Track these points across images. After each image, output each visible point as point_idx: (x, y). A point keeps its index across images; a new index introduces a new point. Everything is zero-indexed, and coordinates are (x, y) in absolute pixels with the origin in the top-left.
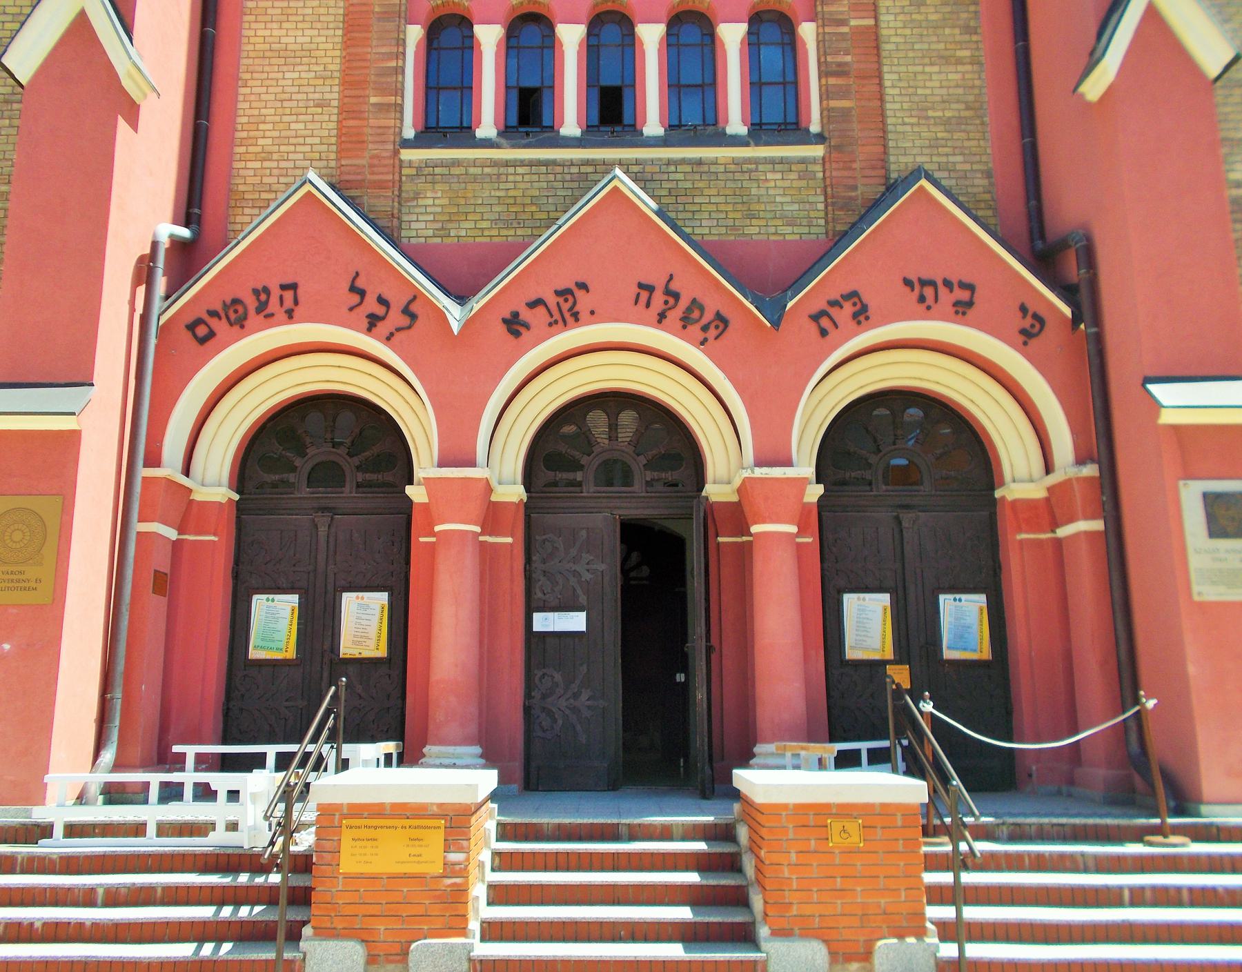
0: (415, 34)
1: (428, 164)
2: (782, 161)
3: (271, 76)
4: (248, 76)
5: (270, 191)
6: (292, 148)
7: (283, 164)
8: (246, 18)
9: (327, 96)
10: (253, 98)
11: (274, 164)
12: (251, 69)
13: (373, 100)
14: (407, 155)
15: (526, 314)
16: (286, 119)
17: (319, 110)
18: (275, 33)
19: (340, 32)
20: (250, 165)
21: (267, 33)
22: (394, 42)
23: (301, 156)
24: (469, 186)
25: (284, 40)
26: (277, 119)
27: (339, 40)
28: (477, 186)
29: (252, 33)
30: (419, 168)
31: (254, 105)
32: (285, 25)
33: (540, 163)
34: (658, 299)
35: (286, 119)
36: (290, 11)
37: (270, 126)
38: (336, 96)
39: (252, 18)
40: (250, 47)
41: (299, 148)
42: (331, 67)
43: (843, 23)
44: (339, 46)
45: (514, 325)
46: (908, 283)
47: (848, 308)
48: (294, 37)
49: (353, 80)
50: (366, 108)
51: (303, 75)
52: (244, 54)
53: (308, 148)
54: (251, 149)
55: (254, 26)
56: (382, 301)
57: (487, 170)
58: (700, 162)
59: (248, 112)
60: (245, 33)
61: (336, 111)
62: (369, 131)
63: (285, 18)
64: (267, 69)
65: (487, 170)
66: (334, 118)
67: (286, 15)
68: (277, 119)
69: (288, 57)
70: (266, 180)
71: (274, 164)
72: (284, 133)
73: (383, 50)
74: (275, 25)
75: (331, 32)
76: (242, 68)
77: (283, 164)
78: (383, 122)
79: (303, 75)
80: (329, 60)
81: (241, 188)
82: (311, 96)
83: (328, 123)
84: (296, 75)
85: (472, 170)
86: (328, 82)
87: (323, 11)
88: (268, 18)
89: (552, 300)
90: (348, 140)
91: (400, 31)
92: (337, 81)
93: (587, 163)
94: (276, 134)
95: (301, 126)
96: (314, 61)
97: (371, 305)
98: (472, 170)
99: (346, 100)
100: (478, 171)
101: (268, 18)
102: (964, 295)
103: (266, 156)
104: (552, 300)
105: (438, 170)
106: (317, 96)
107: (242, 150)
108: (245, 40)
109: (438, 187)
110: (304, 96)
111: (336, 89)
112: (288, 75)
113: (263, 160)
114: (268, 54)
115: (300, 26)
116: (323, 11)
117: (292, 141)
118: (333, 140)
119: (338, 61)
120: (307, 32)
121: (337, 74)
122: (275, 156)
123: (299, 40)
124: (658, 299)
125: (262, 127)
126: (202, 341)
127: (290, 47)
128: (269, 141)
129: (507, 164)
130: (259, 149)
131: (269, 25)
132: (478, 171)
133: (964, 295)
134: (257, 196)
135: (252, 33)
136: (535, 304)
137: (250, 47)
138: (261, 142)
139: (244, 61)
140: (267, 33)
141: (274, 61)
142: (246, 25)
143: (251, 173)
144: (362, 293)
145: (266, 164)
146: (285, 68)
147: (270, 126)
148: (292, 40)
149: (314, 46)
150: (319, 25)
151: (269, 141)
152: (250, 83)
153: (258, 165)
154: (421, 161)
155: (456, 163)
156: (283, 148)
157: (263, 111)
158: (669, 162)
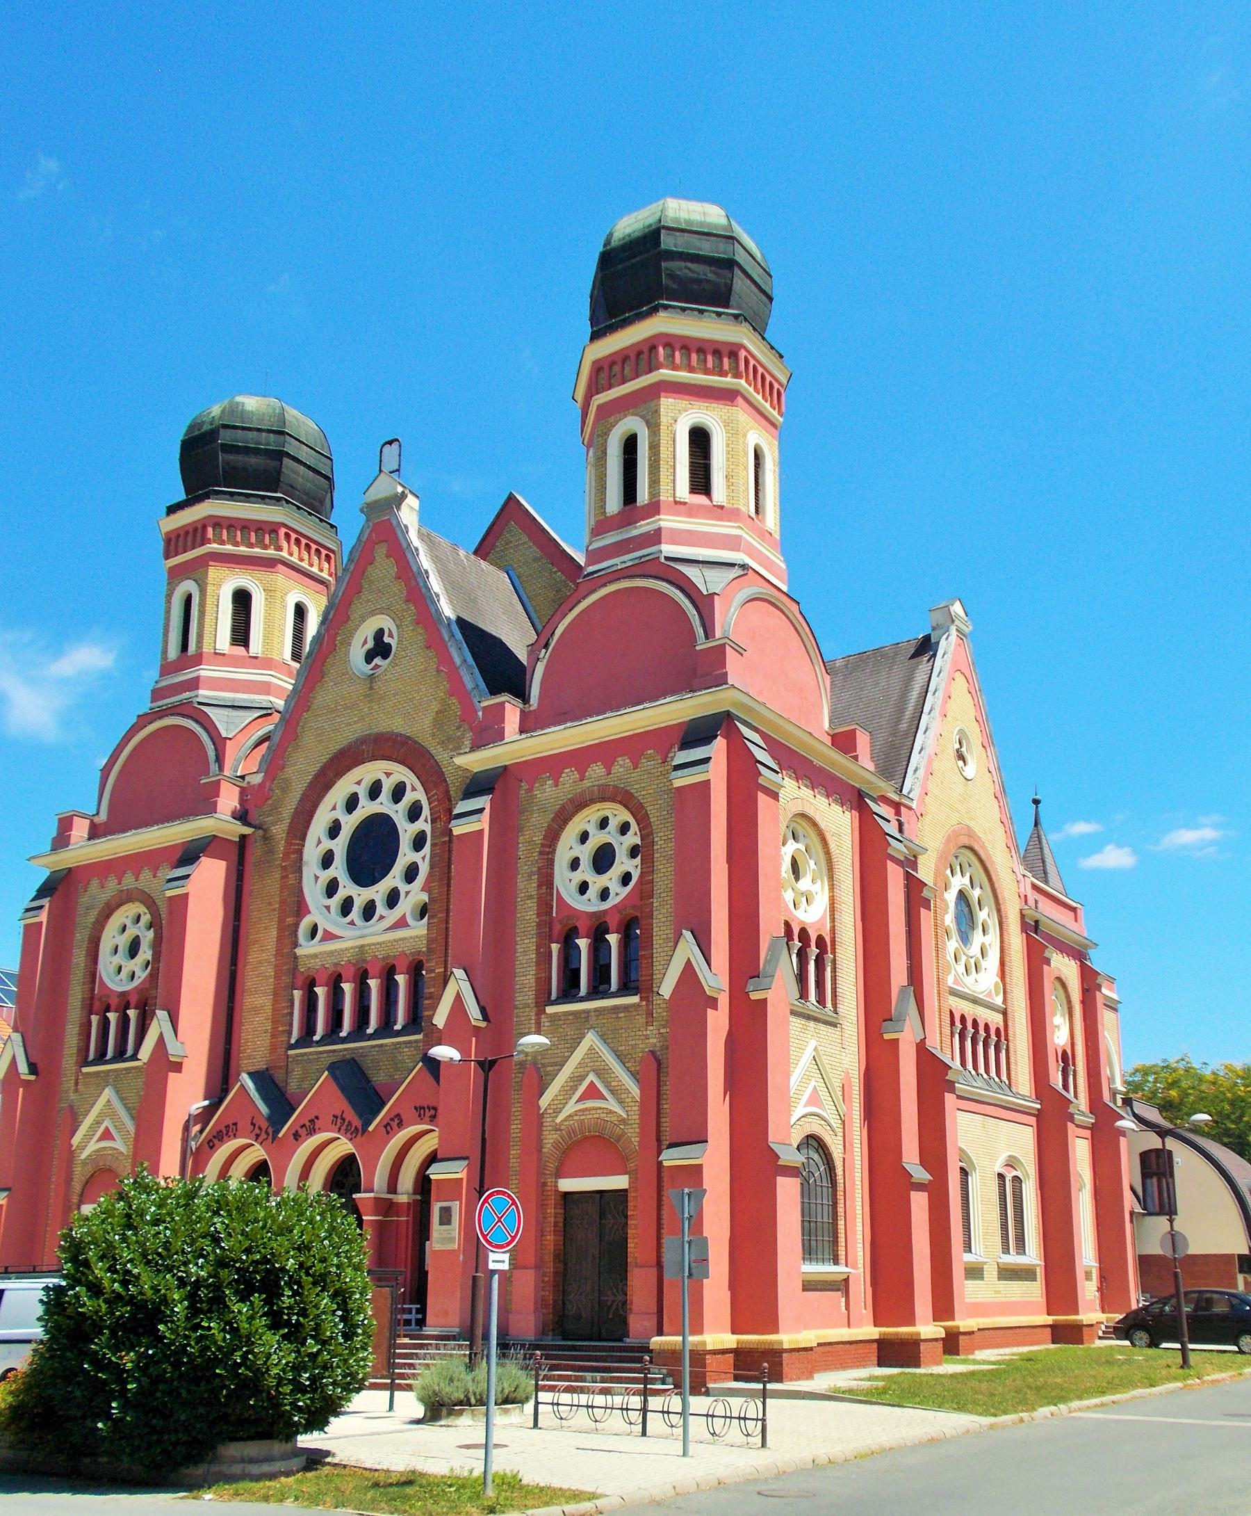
2: (410, 1042)
14: (291, 1052)
15: (300, 1131)
33: (331, 1051)
34: (339, 1121)
43: (433, 971)
45: (297, 1136)
46: (416, 1108)
47: (397, 1121)
56: (260, 1129)
58: (381, 1046)
89: (308, 1124)
93: (345, 1050)
97: (257, 1131)
102: (433, 1112)
103: (249, 1057)
104: (308, 1124)
124: (339, 1121)
126: (211, 1148)
129: (321, 1053)
133: (433, 1112)
136: (304, 1126)
144: (254, 1125)
155: (305, 1054)
158: (372, 1047)
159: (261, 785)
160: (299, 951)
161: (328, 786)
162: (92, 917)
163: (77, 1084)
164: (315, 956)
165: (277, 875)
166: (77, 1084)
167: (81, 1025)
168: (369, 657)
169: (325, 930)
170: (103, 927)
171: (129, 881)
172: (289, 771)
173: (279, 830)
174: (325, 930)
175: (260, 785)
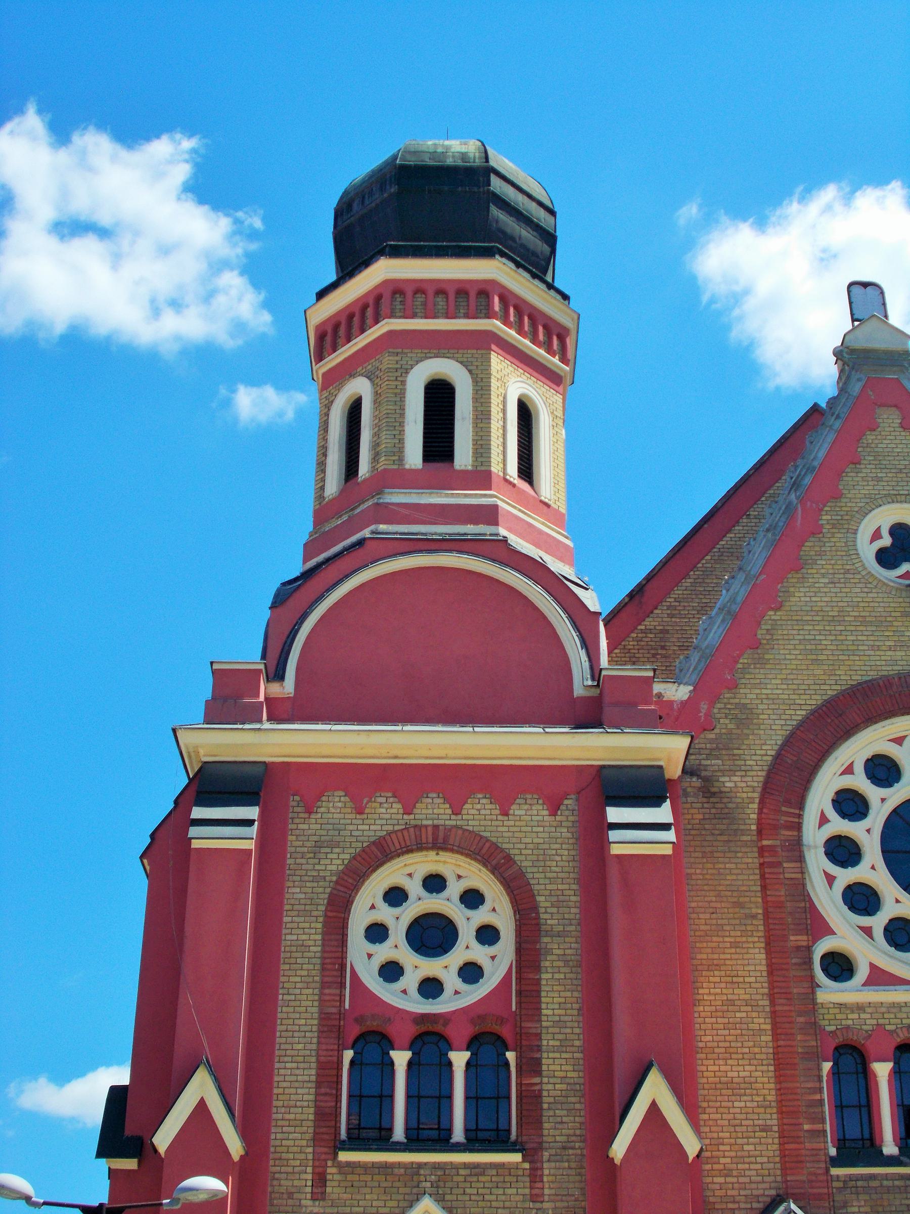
0: (827, 1066)
1: (851, 1178)
3: (723, 1104)
4: (705, 1104)
5: (734, 1202)
6: (747, 1166)
7: (742, 1180)
8: (699, 1056)
9: (769, 1122)
10: (711, 1123)
11: (735, 1180)
12: (707, 1098)
13: (806, 1127)
14: (835, 1171)
16: (739, 1141)
17: (764, 1134)
18: (722, 1068)
19: (772, 1068)
20: (716, 1180)
21: (716, 1068)
22: (816, 1078)
23: (754, 1173)
24: (885, 1196)
25: (729, 1074)
26: (733, 1141)
27: (771, 1074)
28: (891, 1197)
29: (704, 1068)
30: (844, 1181)
31: (713, 1129)
32: (729, 1062)
35: (739, 1141)
36: (732, 1050)
37: (728, 1148)
38: (775, 1122)
39: (703, 1056)
40: (705, 1080)
41: (752, 1166)
42: (769, 1098)
44: (772, 1080)
48: (738, 1072)
49: (788, 1108)
50: (801, 1134)
51: (748, 1104)
52: (700, 1086)
53: (759, 1166)
54: (716, 1166)
55: (705, 1062)
57: (897, 1183)
59: (709, 1135)
60: (700, 1068)
61: (777, 1135)
62: (808, 1152)
63: (728, 1055)
64: (719, 1098)
65: (897, 1183)
66: (776, 1141)
67: (729, 1053)
68: (733, 1141)
69: (734, 1088)
70: (730, 1193)
71: (735, 1180)
72: (739, 1154)
73: (809, 1085)
74: (721, 1062)
75: (765, 1068)
76: (701, 1098)
77: (742, 1180)
78: (815, 1146)
79: (748, 1104)
80: (766, 1092)
81: (712, 1199)
82: (756, 1122)
83: (771, 1146)
84: (743, 1104)
85: (885, 1183)
86: (768, 1110)
87: (756, 1050)
88: (715, 1056)
90: (789, 1160)
91: (819, 1069)
92: (775, 1110)
94: (733, 1154)
95: (751, 1147)
96: (755, 1092)
98: (885, 1183)
99: (785, 1127)
100: (889, 1183)
101: (715, 1056)
105: (860, 1183)
106: (760, 1122)
107: (708, 1167)
108: (700, 1074)
109: (861, 1197)
110: (751, 1122)
111: (775, 1116)
112: (736, 1104)
113: (726, 1176)
114: (718, 1086)
115: (741, 1062)
116: (756, 1050)
117: (746, 1160)
118: (778, 1159)
119: (773, 1092)
120: (747, 1068)
121: (773, 1104)
122: (735, 1173)
123: (741, 1074)
125: (722, 1148)
127: (735, 1080)
128: (728, 1160)
130: (721, 1167)
131: (717, 1062)
132: (889, 1183)
134: (724, 1207)
135: (704, 1068)
137: (705, 1080)
138: (722, 1160)
139: (701, 1092)
140: (716, 1068)
141: (724, 1092)
142: (700, 1062)
143: (717, 1187)
145: (729, 1179)
146: (733, 1098)
147: (728, 1148)
148: (736, 1074)
149: (753, 1080)
150: (755, 1062)
151: (728, 1160)
152: (708, 1110)
153: (721, 1180)
154: (846, 1175)
155: (873, 1177)
156: (740, 1166)
157: (721, 1134)
159: (688, 705)
160: (822, 997)
161: (848, 733)
162: (335, 862)
163: (320, 1179)
164: (860, 1008)
165: (752, 859)
166: (320, 1179)
167: (322, 1066)
168: (886, 558)
169: (873, 967)
170: (355, 888)
171: (433, 811)
172: (747, 695)
173: (744, 784)
174: (873, 967)
175: (684, 704)
